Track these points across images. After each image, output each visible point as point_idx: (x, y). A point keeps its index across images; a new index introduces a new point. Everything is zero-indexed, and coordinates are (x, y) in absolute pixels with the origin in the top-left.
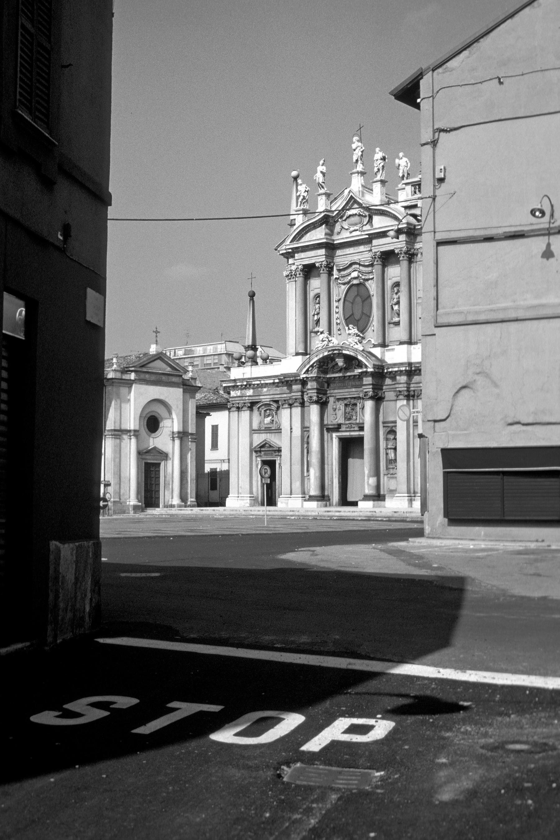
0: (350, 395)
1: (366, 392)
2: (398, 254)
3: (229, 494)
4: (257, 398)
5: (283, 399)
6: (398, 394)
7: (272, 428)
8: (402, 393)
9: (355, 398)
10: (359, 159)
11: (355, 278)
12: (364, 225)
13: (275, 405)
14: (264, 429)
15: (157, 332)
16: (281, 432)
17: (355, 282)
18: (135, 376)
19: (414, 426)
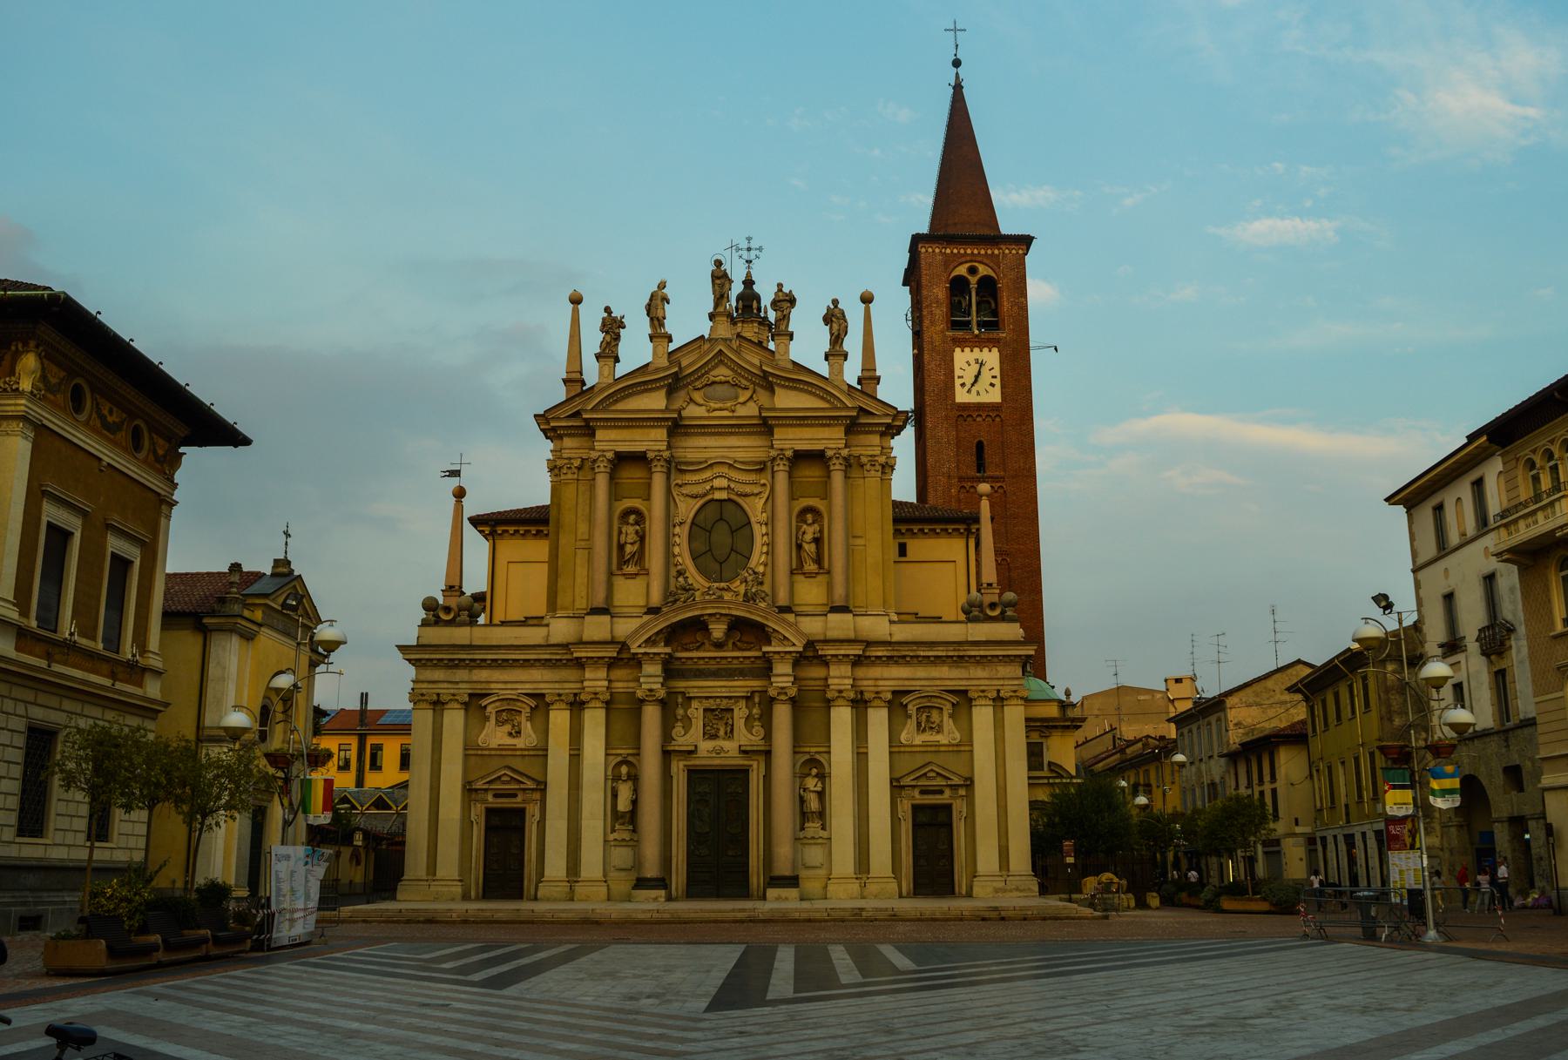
0: (730, 692)
1: (783, 688)
2: (830, 458)
3: (403, 875)
4: (483, 686)
5: (557, 691)
6: (837, 694)
7: (518, 747)
8: (844, 695)
9: (730, 698)
10: (726, 295)
11: (720, 489)
12: (739, 403)
13: (533, 703)
14: (497, 747)
15: (287, 535)
16: (547, 755)
17: (723, 495)
18: (262, 618)
19: (858, 753)
